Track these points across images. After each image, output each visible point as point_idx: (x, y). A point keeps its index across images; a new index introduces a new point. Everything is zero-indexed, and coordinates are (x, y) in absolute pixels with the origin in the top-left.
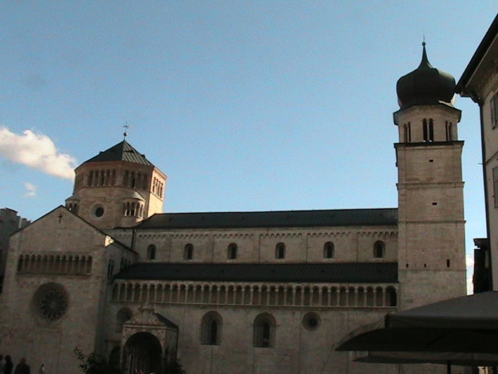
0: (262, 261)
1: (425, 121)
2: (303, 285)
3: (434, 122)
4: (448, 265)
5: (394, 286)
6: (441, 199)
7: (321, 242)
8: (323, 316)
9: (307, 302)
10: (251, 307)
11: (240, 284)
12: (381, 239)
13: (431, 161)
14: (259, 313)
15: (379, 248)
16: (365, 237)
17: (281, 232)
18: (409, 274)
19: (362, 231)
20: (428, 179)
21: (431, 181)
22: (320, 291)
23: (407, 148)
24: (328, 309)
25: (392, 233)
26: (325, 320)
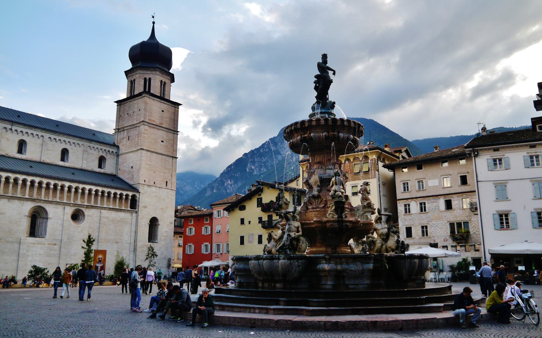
0: (4, 154)
1: (161, 81)
2: (74, 185)
3: (166, 85)
4: (166, 186)
5: (136, 194)
6: (166, 140)
7: (59, 147)
8: (87, 212)
9: (76, 198)
10: (27, 199)
11: (18, 176)
12: (104, 155)
13: (163, 111)
14: (34, 206)
15: (102, 161)
16: (93, 151)
17: (25, 130)
18: (146, 186)
19: (92, 145)
20: (161, 123)
21: (162, 126)
22: (87, 192)
23: (151, 97)
24: (92, 207)
25: (112, 152)
26: (88, 216)
